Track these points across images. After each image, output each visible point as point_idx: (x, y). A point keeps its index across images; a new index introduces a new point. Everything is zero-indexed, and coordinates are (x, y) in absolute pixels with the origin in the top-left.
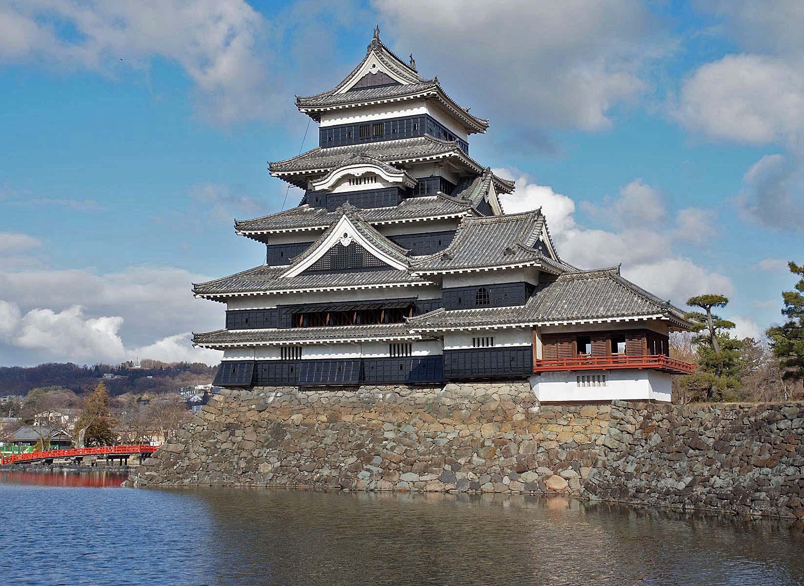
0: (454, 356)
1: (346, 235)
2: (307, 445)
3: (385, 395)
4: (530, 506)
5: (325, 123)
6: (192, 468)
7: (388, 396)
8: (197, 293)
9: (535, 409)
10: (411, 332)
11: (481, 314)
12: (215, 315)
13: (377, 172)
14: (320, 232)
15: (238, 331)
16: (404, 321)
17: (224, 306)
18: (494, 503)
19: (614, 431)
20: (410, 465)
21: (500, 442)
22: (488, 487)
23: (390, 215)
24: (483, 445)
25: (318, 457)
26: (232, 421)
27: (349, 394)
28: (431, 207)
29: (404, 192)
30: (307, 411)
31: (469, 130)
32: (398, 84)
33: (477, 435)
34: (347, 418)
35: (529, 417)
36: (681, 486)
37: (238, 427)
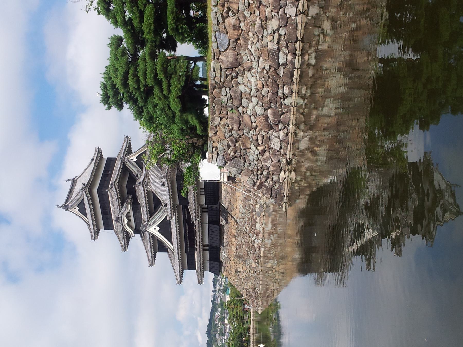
1: (155, 229)
6: (254, 289)
8: (180, 283)
12: (191, 276)
13: (125, 213)
17: (186, 271)
20: (253, 225)
25: (249, 245)
26: (234, 271)
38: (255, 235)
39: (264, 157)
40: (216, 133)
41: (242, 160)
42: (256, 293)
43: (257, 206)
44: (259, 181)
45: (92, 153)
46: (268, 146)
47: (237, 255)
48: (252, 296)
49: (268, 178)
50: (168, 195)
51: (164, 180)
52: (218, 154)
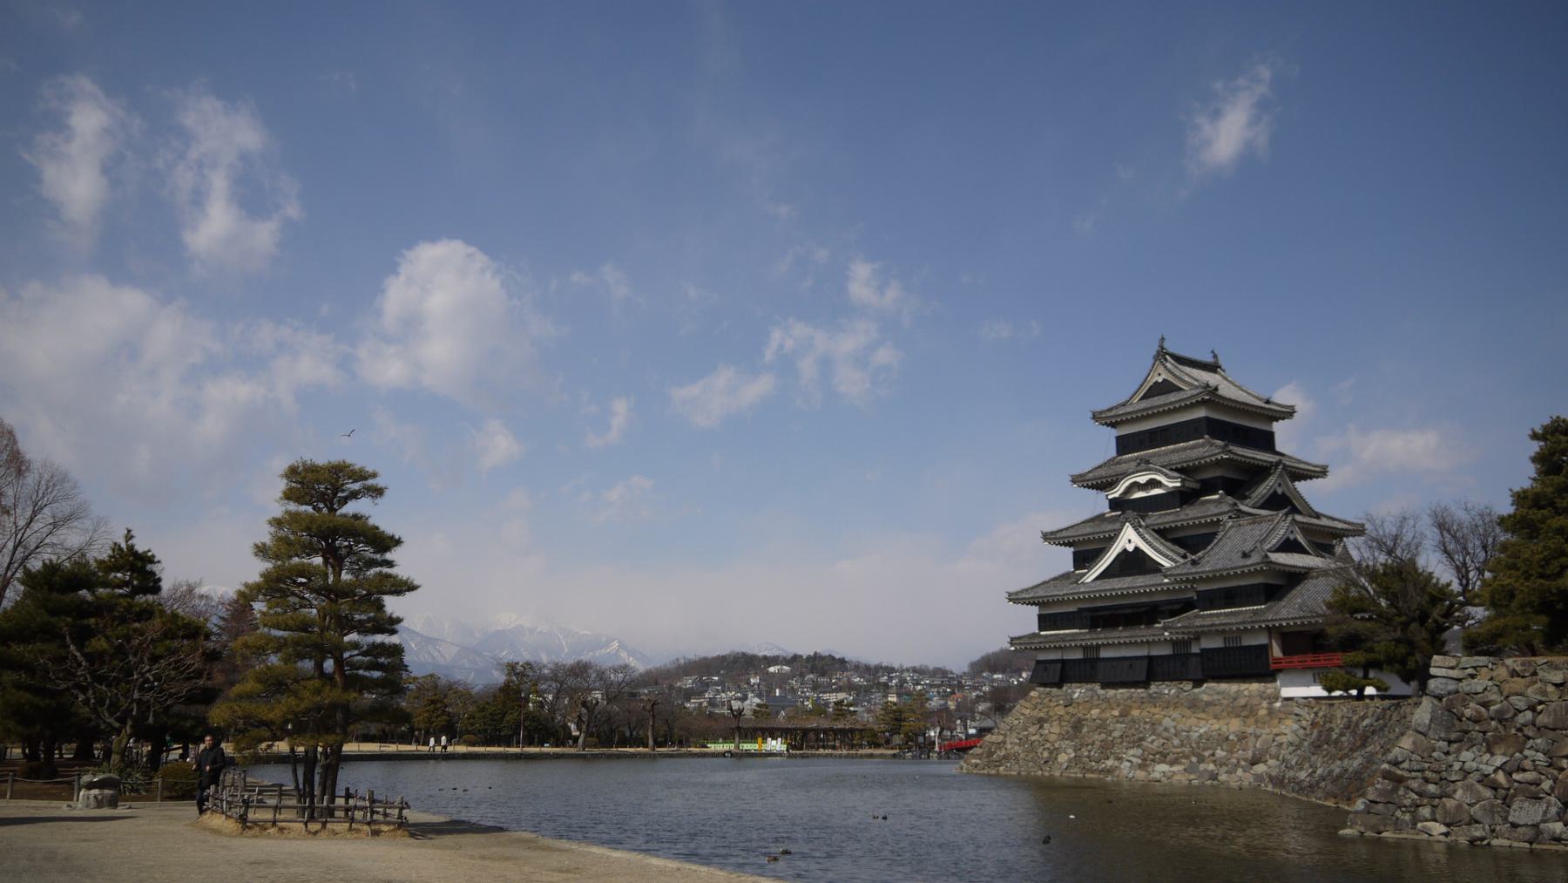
2: (1098, 737)
6: (1006, 757)
9: (1278, 704)
12: (1026, 620)
17: (1035, 610)
20: (1164, 757)
25: (1107, 749)
28: (1215, 504)
33: (1224, 729)
34: (1135, 713)
35: (1271, 712)
39: (1480, 787)
40: (1514, 673)
41: (1453, 736)
42: (1000, 762)
43: (1211, 767)
44: (1406, 774)
45: (1282, 397)
46: (1514, 796)
47: (1080, 720)
48: (991, 754)
49: (1420, 795)
50: (1220, 566)
51: (1255, 558)
52: (1460, 680)
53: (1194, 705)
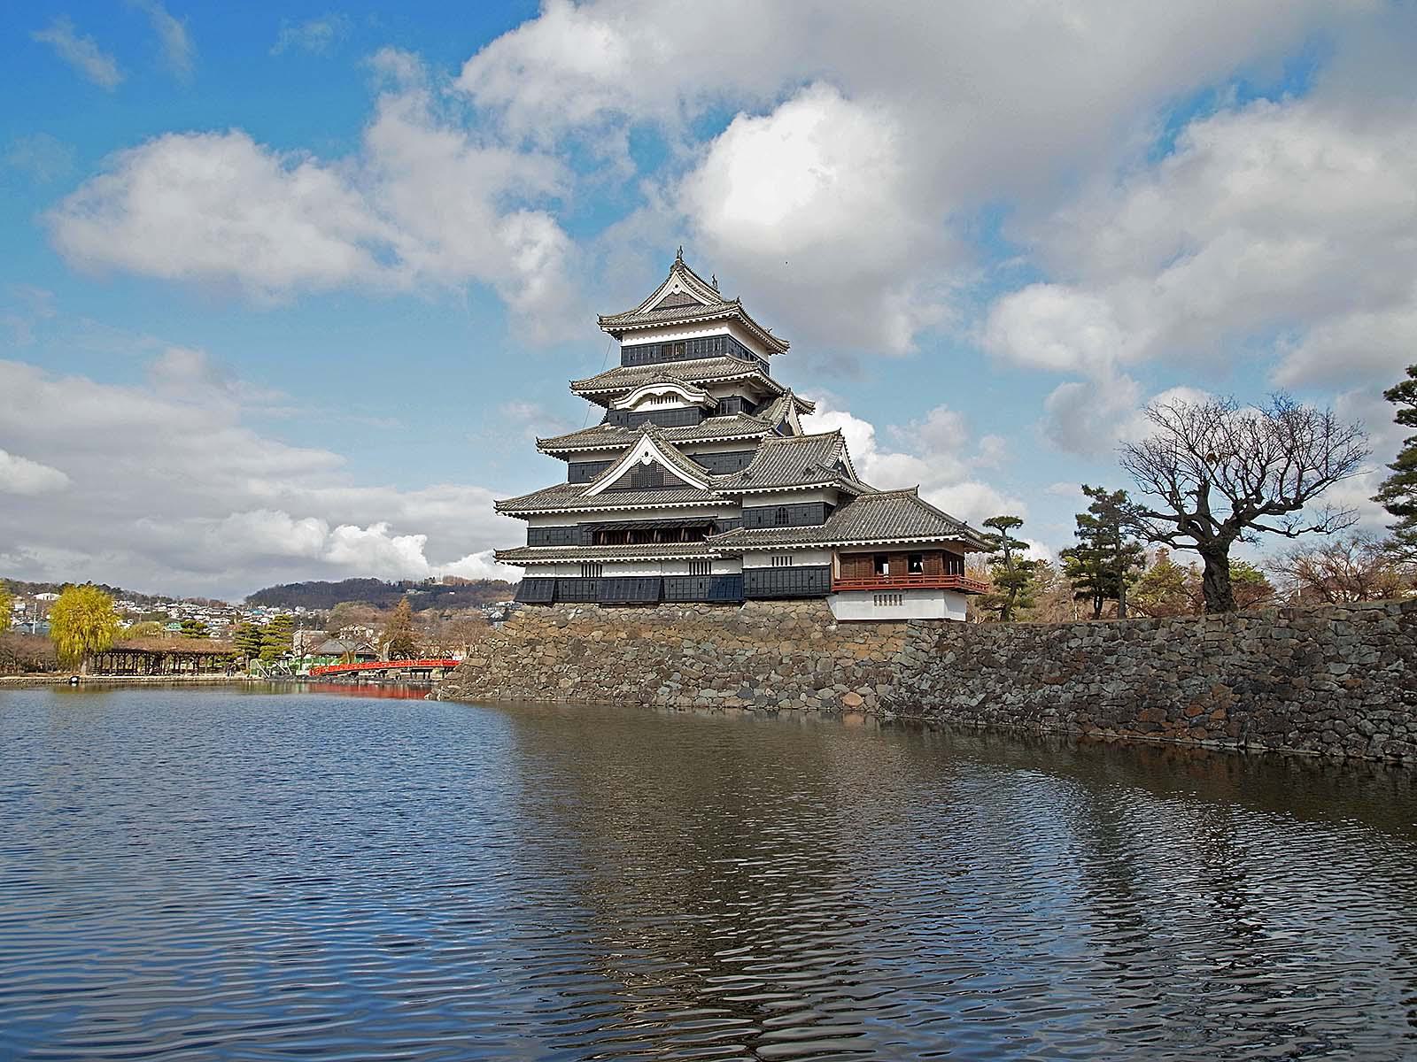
0: (754, 575)
1: (647, 454)
3: (684, 613)
4: (826, 721)
5: (627, 342)
6: (494, 682)
7: (688, 613)
8: (499, 510)
10: (711, 551)
11: (780, 533)
12: (517, 533)
13: (678, 391)
14: (622, 450)
15: (539, 548)
16: (704, 539)
18: (791, 718)
19: (910, 649)
21: (798, 660)
22: (785, 703)
23: (690, 434)
24: (781, 663)
25: (618, 674)
26: (533, 637)
27: (648, 611)
28: (733, 425)
29: (707, 412)
30: (606, 628)
31: (770, 350)
32: (700, 304)
33: (775, 652)
34: (647, 635)
35: (826, 635)
36: (974, 703)
37: (539, 643)
38: (680, 687)
53: (733, 626)
